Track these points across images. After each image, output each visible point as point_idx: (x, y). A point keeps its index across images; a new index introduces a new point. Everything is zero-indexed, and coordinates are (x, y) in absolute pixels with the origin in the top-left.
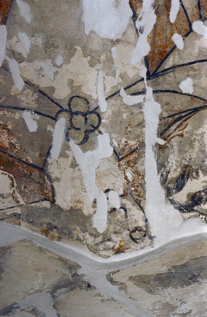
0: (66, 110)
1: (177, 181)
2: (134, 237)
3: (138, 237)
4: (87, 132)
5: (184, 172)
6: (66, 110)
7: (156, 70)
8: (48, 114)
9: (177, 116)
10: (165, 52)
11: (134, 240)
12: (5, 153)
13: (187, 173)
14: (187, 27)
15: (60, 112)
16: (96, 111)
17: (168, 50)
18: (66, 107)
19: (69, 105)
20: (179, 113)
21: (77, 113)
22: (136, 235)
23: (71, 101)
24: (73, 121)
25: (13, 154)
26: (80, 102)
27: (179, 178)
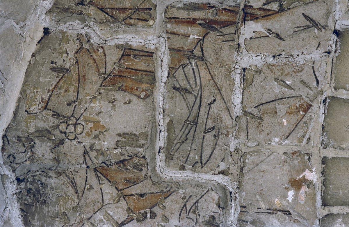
0: (76, 122)
1: (40, 181)
2: (10, 157)
3: (10, 159)
4: (65, 133)
5: (44, 185)
6: (76, 122)
7: (98, 171)
8: (75, 112)
9: (73, 182)
10: (107, 176)
11: (8, 157)
12: (54, 88)
13: (44, 186)
14: (120, 188)
15: (76, 119)
16: (76, 138)
17: (108, 178)
18: (78, 122)
19: (79, 124)
20: (75, 183)
21: (75, 128)
22: (11, 158)
23: (81, 124)
24: (71, 126)
25: (54, 92)
26: (81, 130)
27: (41, 182)
